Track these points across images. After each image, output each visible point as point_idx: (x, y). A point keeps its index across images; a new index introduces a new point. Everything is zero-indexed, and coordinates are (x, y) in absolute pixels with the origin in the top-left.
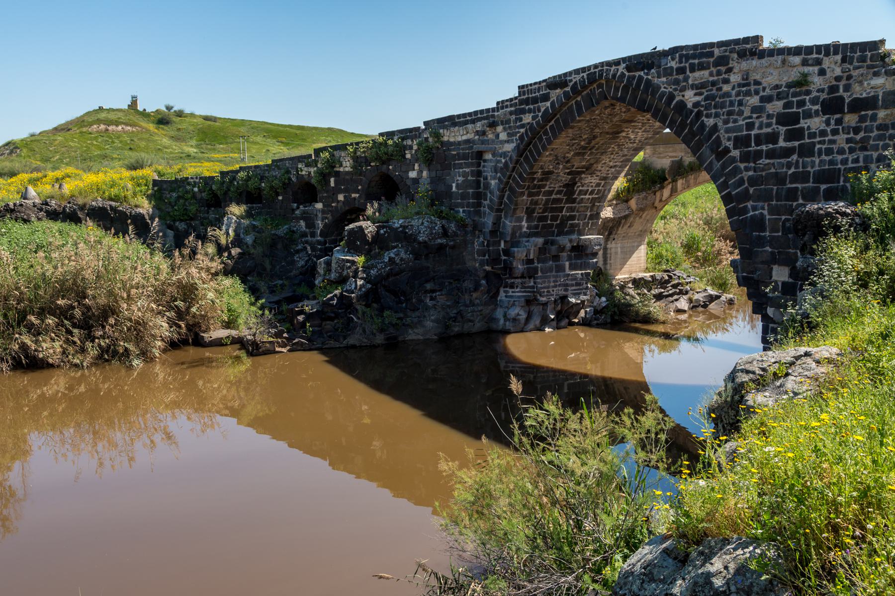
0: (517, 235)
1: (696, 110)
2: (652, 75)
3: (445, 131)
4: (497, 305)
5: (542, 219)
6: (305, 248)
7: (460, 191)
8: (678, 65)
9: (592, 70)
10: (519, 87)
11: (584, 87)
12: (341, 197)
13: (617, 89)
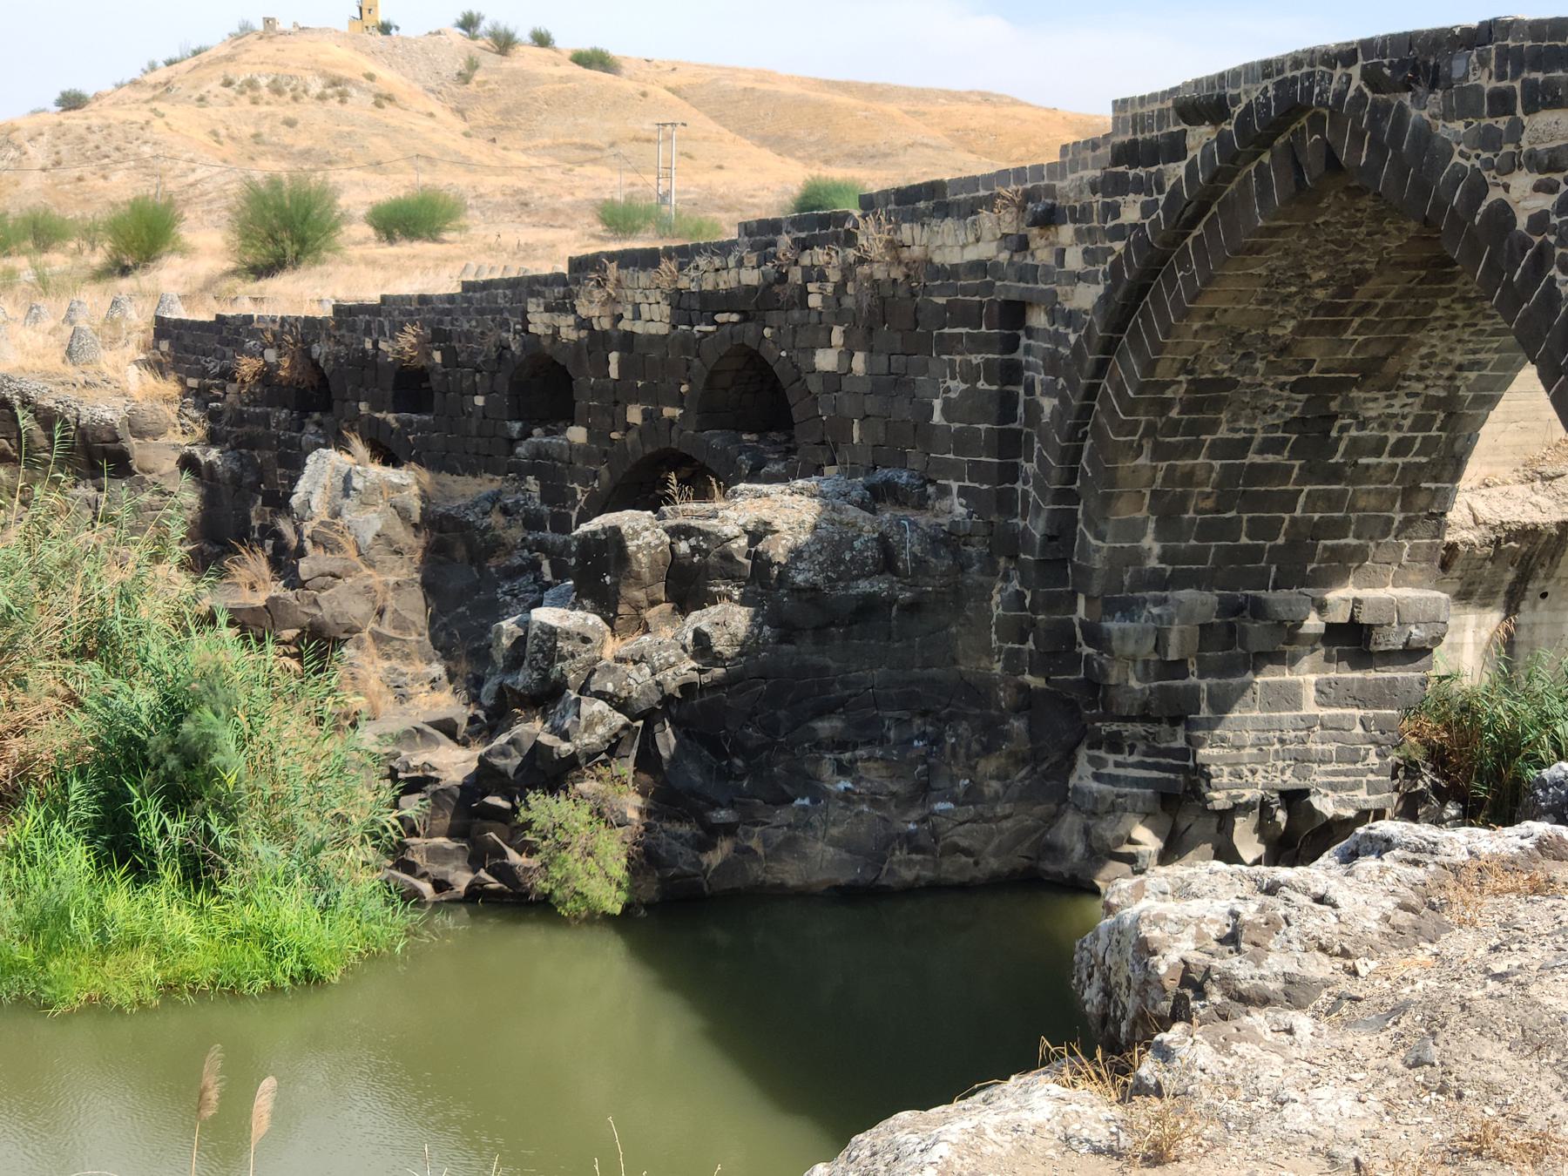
0: (1127, 579)
1: (1537, 240)
2: (1422, 109)
3: (917, 228)
4: (1066, 800)
5: (1208, 530)
6: (536, 566)
7: (955, 426)
8: (1494, 83)
9: (1288, 74)
10: (1115, 102)
11: (1277, 127)
12: (634, 415)
13: (1358, 137)
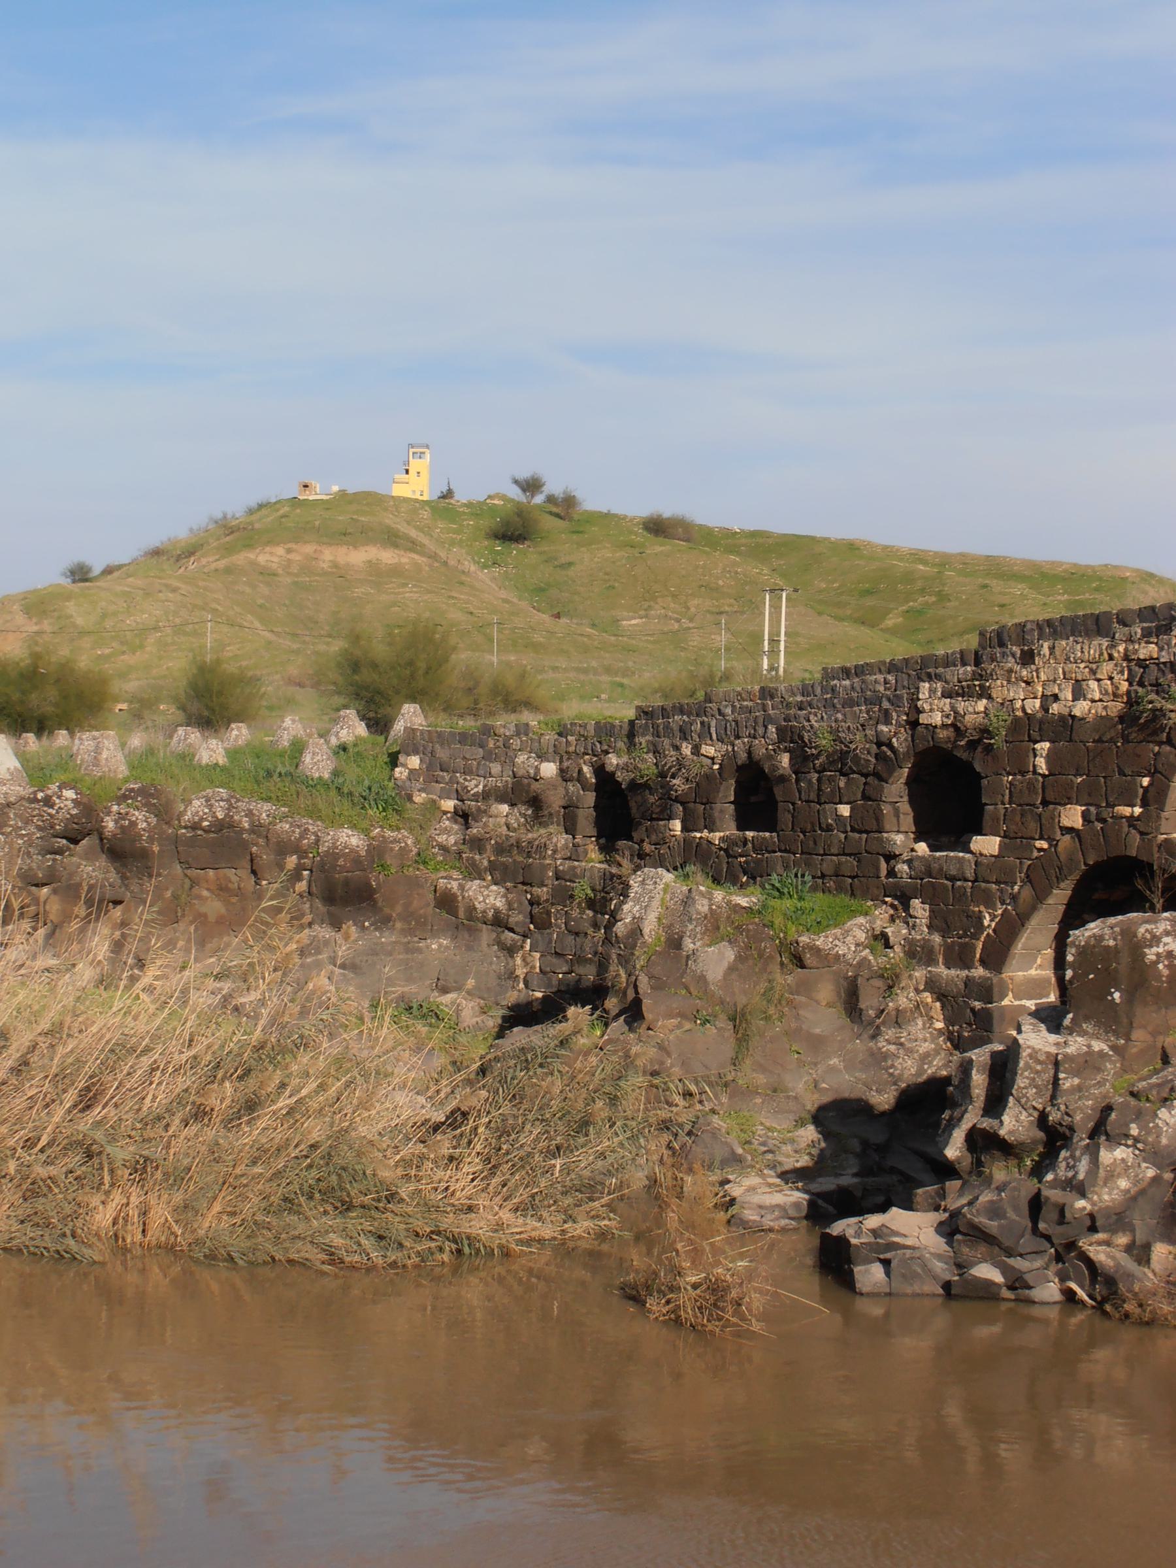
12: (1073, 816)
